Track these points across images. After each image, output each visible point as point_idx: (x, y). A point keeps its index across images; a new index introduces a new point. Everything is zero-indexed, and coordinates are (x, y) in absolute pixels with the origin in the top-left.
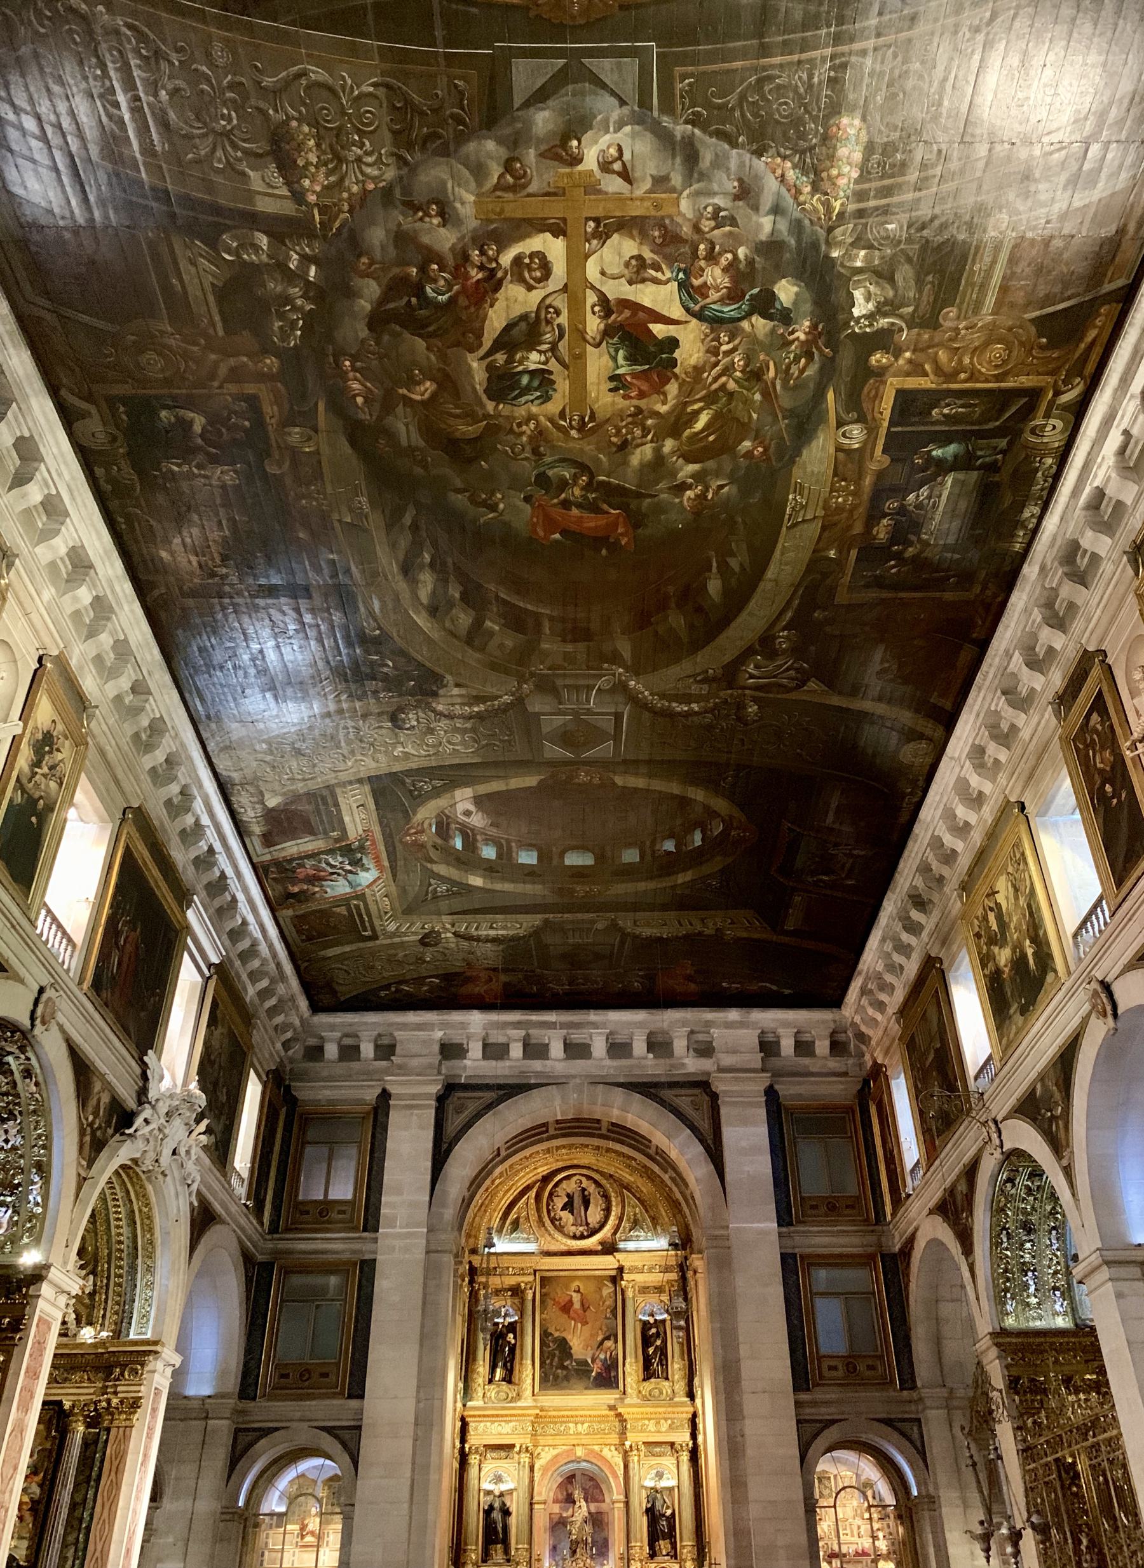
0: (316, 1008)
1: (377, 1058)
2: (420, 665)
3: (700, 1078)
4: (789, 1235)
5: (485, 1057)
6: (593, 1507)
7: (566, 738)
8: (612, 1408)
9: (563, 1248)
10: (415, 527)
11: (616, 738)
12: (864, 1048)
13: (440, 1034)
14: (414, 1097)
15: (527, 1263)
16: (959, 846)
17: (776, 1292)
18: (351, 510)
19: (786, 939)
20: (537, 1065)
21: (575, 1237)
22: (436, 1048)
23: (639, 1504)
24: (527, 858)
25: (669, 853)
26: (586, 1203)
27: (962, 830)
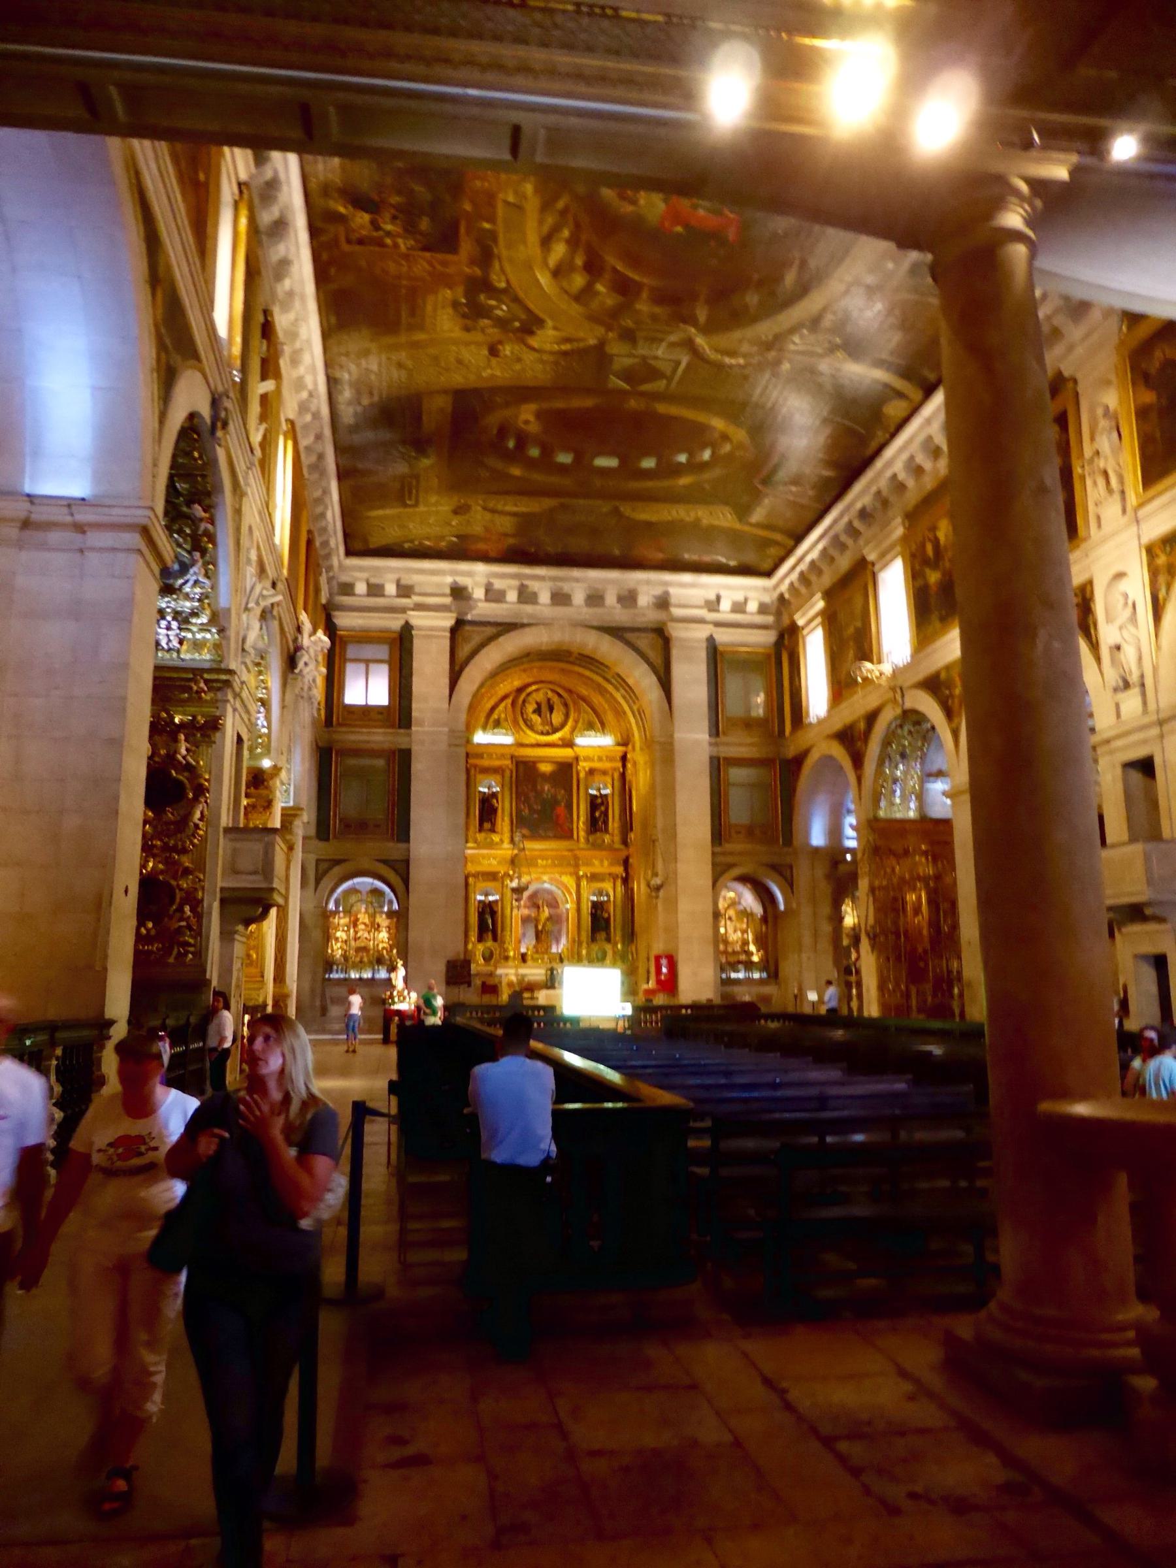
0: (349, 553)
1: (399, 596)
2: (528, 310)
3: (654, 626)
4: (716, 744)
5: (487, 600)
6: (553, 911)
7: (628, 376)
8: (571, 850)
9: (533, 741)
10: (564, 213)
11: (670, 379)
12: (783, 609)
13: (449, 580)
14: (432, 629)
15: (508, 751)
16: (911, 483)
17: (704, 783)
18: (516, 193)
19: (747, 528)
20: (529, 608)
21: (542, 733)
22: (448, 591)
23: (586, 909)
24: (565, 458)
25: (680, 464)
26: (551, 709)
27: (918, 471)
